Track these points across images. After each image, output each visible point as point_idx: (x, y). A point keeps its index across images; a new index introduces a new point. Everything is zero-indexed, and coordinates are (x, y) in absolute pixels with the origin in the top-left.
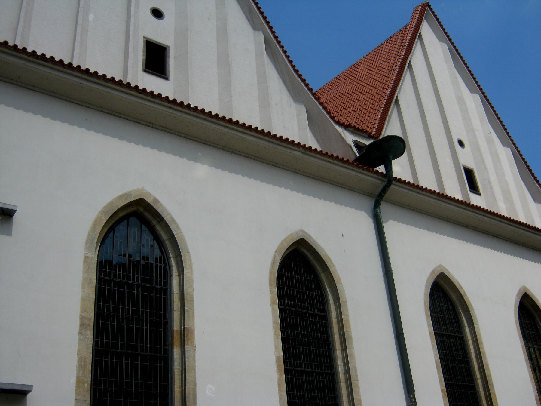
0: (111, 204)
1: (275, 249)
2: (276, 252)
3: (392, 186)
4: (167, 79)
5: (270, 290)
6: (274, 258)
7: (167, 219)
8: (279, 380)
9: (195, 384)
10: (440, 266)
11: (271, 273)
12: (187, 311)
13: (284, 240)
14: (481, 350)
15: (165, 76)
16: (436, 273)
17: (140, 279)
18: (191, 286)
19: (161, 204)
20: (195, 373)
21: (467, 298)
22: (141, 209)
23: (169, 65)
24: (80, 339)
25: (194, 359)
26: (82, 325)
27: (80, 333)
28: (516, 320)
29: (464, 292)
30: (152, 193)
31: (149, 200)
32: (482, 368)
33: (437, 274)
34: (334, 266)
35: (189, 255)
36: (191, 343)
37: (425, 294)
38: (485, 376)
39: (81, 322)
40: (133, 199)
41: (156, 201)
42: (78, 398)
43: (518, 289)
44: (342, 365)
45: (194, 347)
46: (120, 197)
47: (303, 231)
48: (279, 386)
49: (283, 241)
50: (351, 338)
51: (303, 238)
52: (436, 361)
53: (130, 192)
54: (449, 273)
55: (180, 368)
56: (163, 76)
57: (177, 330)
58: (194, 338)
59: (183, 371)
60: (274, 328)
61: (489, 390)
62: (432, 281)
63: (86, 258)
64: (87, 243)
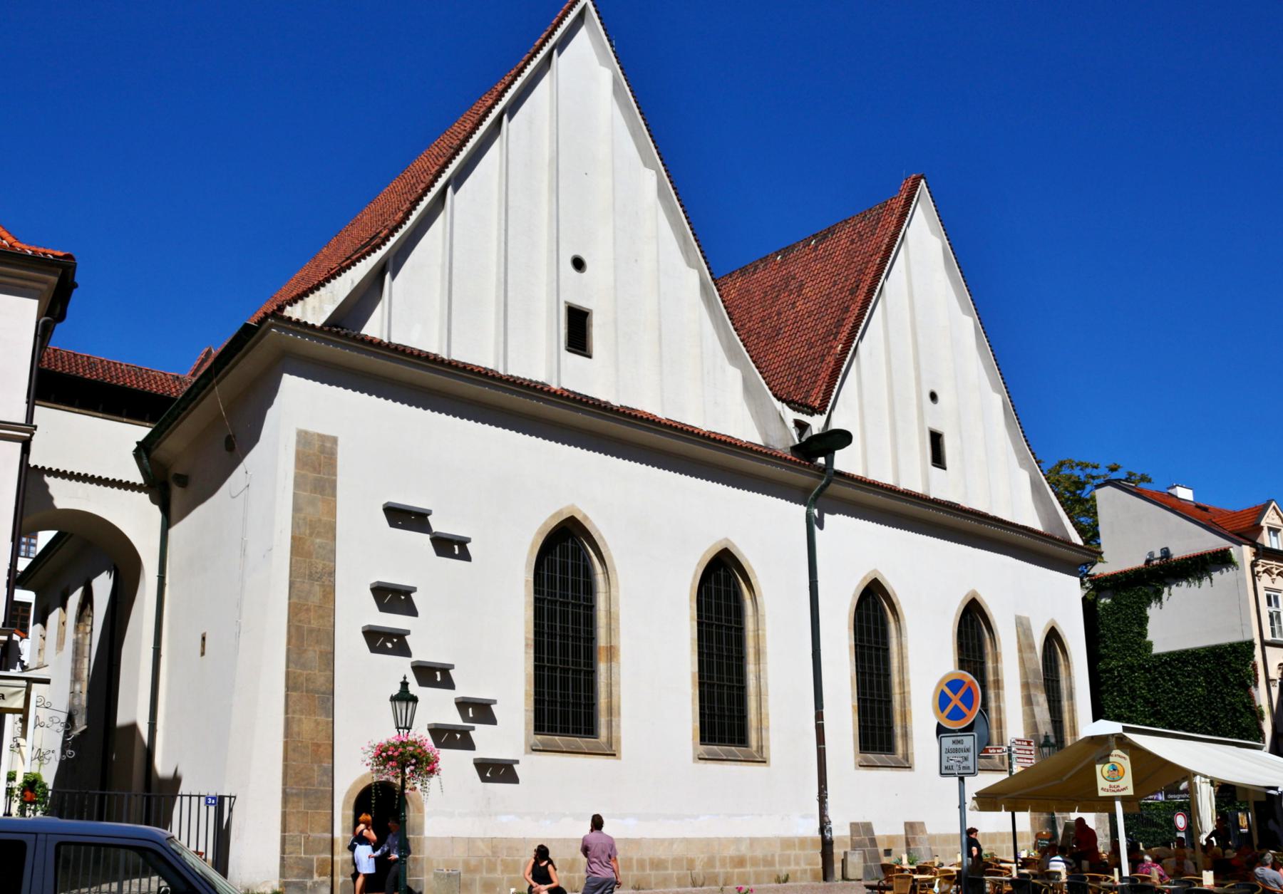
1: (698, 561)
2: (698, 564)
4: (590, 357)
7: (596, 537)
8: (693, 694)
9: (619, 698)
10: (875, 571)
12: (614, 630)
13: (707, 551)
14: (905, 665)
15: (584, 353)
17: (570, 596)
18: (617, 605)
19: (591, 521)
20: (619, 687)
21: (900, 607)
25: (619, 674)
26: (527, 645)
27: (526, 653)
28: (953, 631)
29: (898, 600)
30: (582, 509)
31: (579, 517)
32: (902, 684)
33: (869, 580)
35: (616, 574)
37: (851, 604)
38: (904, 693)
41: (586, 517)
42: (527, 708)
43: (965, 593)
44: (754, 678)
45: (618, 663)
46: (553, 517)
47: (727, 539)
48: (693, 700)
53: (561, 510)
54: (883, 578)
55: (606, 681)
56: (584, 353)
57: (604, 647)
58: (619, 655)
59: (610, 685)
60: (692, 644)
61: (905, 706)
62: (865, 584)
63: (527, 581)
64: (526, 567)
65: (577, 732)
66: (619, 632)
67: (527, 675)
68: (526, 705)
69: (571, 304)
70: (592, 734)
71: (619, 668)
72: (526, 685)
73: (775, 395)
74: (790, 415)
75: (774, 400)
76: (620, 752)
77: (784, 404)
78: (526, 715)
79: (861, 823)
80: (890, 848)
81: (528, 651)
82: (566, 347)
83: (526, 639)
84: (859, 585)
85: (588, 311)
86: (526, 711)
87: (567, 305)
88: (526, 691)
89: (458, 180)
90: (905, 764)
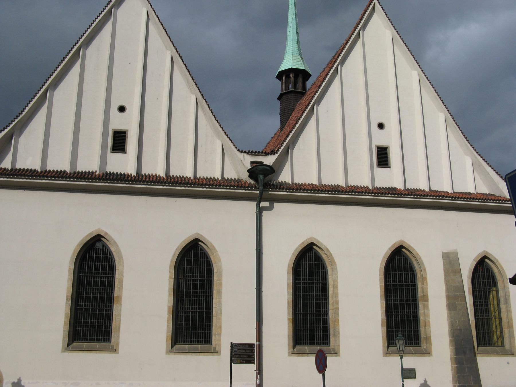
0: (83, 239)
2: (176, 249)
5: (170, 272)
6: (175, 253)
8: (168, 318)
11: (171, 261)
13: (183, 241)
16: (305, 243)
19: (109, 235)
23: (127, 143)
24: (66, 305)
26: (67, 299)
27: (66, 303)
34: (217, 251)
36: (120, 303)
39: (67, 298)
40: (94, 235)
42: (64, 330)
45: (121, 305)
48: (168, 321)
49: (183, 242)
50: (222, 292)
51: (197, 238)
52: (288, 302)
63: (70, 268)
64: (70, 262)
65: (99, 339)
67: (66, 314)
68: (64, 328)
70: (109, 341)
71: (121, 307)
72: (65, 319)
73: (239, 150)
74: (248, 160)
75: (238, 153)
76: (118, 350)
78: (64, 333)
81: (68, 302)
82: (111, 151)
83: (67, 296)
84: (298, 248)
85: (125, 131)
86: (64, 331)
88: (65, 322)
89: (55, 84)
90: (216, 352)
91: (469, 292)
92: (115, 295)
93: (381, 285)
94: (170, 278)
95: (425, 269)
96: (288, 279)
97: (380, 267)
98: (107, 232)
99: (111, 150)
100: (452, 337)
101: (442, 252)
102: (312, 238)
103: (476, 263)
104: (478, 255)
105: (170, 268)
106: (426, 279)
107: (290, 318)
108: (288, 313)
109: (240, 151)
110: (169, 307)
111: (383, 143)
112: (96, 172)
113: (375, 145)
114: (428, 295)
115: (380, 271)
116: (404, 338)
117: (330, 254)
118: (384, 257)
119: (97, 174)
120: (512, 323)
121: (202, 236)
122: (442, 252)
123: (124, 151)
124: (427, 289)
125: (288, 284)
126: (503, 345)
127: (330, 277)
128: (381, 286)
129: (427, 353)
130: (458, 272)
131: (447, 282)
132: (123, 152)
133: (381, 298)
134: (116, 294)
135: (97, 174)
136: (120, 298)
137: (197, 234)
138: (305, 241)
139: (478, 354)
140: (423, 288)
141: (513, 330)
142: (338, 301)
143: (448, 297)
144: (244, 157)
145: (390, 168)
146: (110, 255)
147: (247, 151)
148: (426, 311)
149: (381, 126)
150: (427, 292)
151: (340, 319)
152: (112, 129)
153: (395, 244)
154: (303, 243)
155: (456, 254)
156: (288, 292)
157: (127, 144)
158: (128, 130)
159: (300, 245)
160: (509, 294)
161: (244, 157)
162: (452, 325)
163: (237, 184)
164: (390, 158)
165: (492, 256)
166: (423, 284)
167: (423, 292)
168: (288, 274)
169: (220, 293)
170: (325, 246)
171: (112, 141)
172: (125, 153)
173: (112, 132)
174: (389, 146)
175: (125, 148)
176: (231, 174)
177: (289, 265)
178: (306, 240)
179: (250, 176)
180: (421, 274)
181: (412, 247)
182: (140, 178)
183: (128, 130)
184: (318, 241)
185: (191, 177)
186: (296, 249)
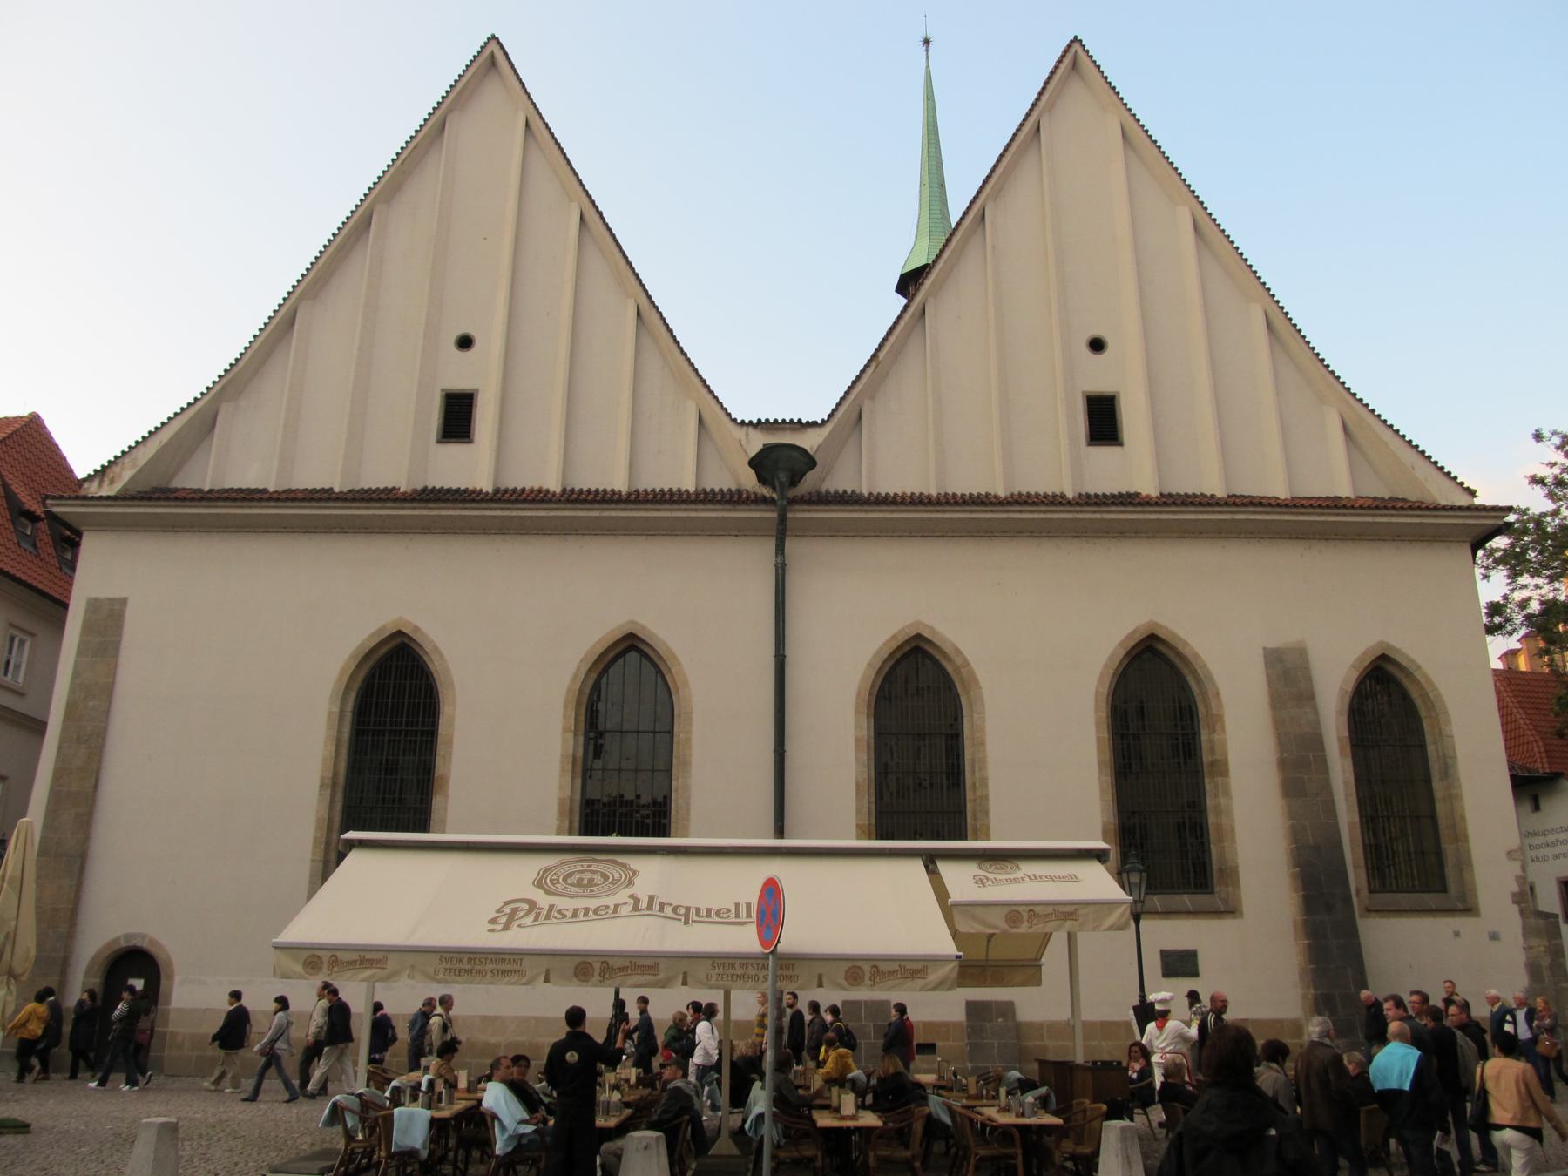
1: (582, 655)
2: (582, 661)
3: (790, 515)
11: (569, 691)
19: (423, 632)
22: (406, 640)
23: (475, 419)
26: (322, 786)
27: (320, 795)
34: (680, 664)
41: (417, 629)
45: (447, 797)
63: (330, 713)
66: (450, 761)
69: (447, 390)
77: (750, 429)
79: (866, 1002)
80: (930, 1041)
83: (322, 778)
86: (313, 861)
87: (444, 393)
88: (315, 838)
91: (1341, 749)
92: (436, 775)
93: (1102, 735)
94: (565, 730)
95: (1218, 694)
96: (857, 727)
97: (1097, 691)
98: (419, 624)
99: (437, 436)
100: (1294, 867)
101: (1264, 649)
102: (919, 623)
103: (1358, 674)
104: (1365, 653)
105: (566, 707)
106: (1220, 718)
107: (861, 822)
108: (858, 811)
109: (739, 421)
110: (561, 802)
111: (1102, 387)
112: (399, 489)
113: (1083, 393)
114: (1226, 760)
115: (1096, 700)
116: (1141, 868)
117: (965, 660)
118: (1106, 666)
119: (401, 491)
120: (1465, 829)
121: (644, 628)
122: (1264, 649)
123: (468, 437)
124: (1224, 743)
125: (857, 740)
126: (1443, 889)
127: (965, 720)
128: (1099, 740)
129: (1230, 910)
130: (1306, 697)
131: (1278, 724)
132: (466, 440)
133: (1100, 771)
134: (439, 770)
135: (401, 491)
136: (445, 779)
137: (632, 622)
138: (900, 631)
139: (1369, 911)
140: (1211, 741)
141: (1469, 847)
142: (987, 779)
143: (1283, 764)
144: (747, 435)
145: (1121, 444)
146: (428, 678)
147: (755, 422)
148: (1222, 801)
149: (1097, 345)
150: (1225, 752)
151: (991, 826)
152: (442, 390)
153: (1134, 632)
154: (894, 637)
155: (1301, 652)
156: (857, 759)
157: (474, 423)
158: (477, 390)
159: (888, 641)
160: (1455, 752)
161: (747, 435)
162: (1296, 835)
163: (735, 498)
164: (1121, 422)
165: (1404, 655)
166: (1214, 732)
167: (1212, 750)
168: (856, 713)
169: (686, 764)
170: (950, 642)
171: (442, 415)
172: (471, 442)
173: (441, 396)
174: (1118, 393)
175: (469, 432)
176: (719, 481)
177: (859, 693)
178: (903, 629)
179: (762, 479)
180: (1208, 707)
181: (1180, 639)
182: (503, 497)
183: (477, 390)
184: (932, 629)
185: (622, 489)
186: (878, 652)
